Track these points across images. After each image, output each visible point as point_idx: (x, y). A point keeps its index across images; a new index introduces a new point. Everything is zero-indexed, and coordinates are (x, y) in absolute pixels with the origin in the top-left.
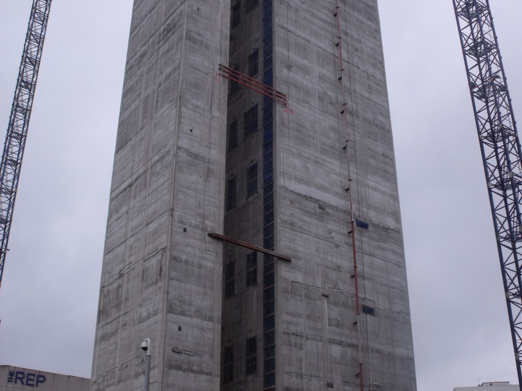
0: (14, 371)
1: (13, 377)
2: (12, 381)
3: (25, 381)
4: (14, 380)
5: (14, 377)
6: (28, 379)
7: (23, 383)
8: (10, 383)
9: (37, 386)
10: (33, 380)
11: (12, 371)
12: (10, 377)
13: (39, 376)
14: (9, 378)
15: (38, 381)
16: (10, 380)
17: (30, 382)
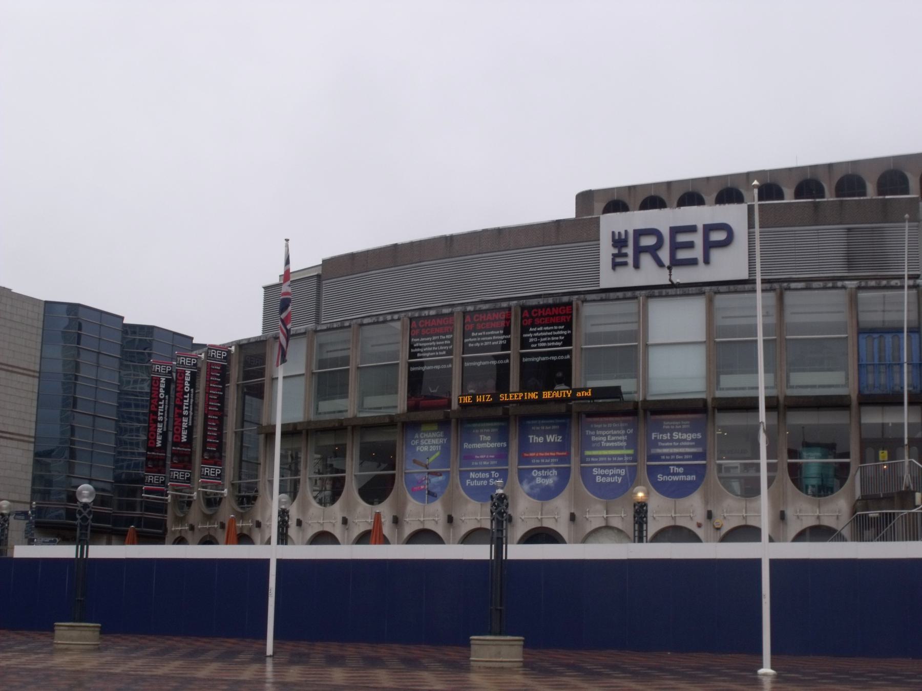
0: (626, 232)
1: (624, 251)
2: (625, 264)
3: (664, 254)
4: (630, 260)
5: (630, 250)
6: (675, 247)
7: (660, 264)
9: (707, 261)
10: (690, 245)
12: (616, 251)
13: (709, 229)
14: (614, 256)
15: (709, 246)
16: (618, 260)
17: (682, 255)
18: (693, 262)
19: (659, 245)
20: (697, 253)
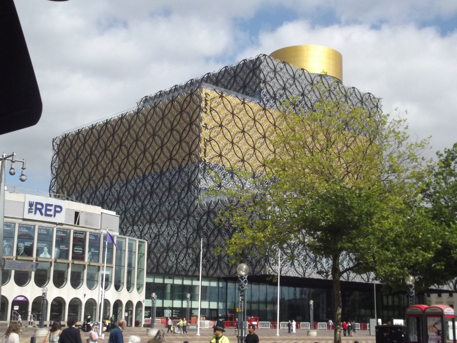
1: (32, 208)
2: (32, 212)
3: (43, 211)
4: (34, 210)
5: (34, 208)
6: (47, 210)
7: (42, 214)
8: (30, 214)
9: (55, 216)
11: (31, 202)
12: (30, 208)
13: (56, 206)
14: (29, 209)
15: (56, 212)
16: (30, 211)
17: (48, 213)
18: (50, 216)
19: (42, 208)
20: (52, 213)
